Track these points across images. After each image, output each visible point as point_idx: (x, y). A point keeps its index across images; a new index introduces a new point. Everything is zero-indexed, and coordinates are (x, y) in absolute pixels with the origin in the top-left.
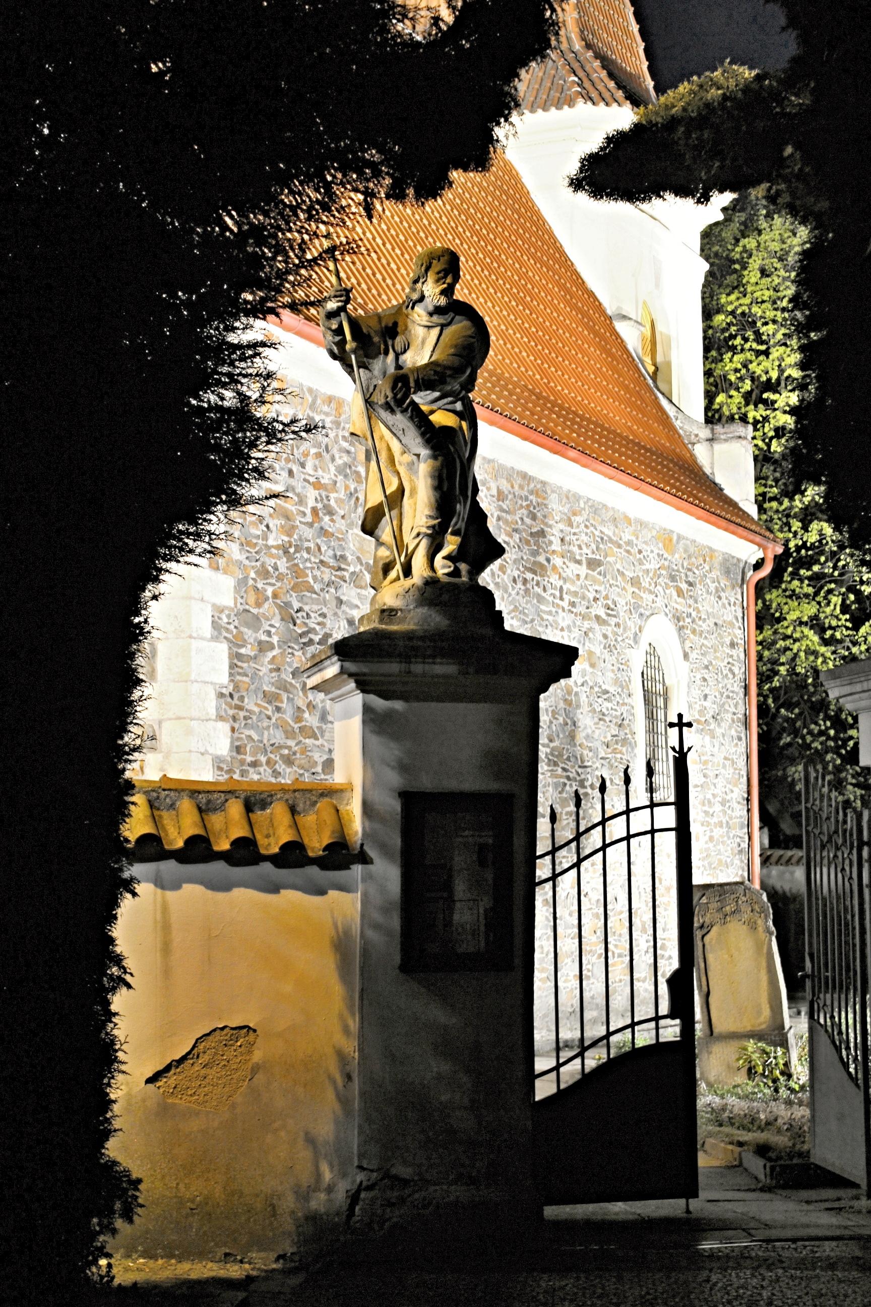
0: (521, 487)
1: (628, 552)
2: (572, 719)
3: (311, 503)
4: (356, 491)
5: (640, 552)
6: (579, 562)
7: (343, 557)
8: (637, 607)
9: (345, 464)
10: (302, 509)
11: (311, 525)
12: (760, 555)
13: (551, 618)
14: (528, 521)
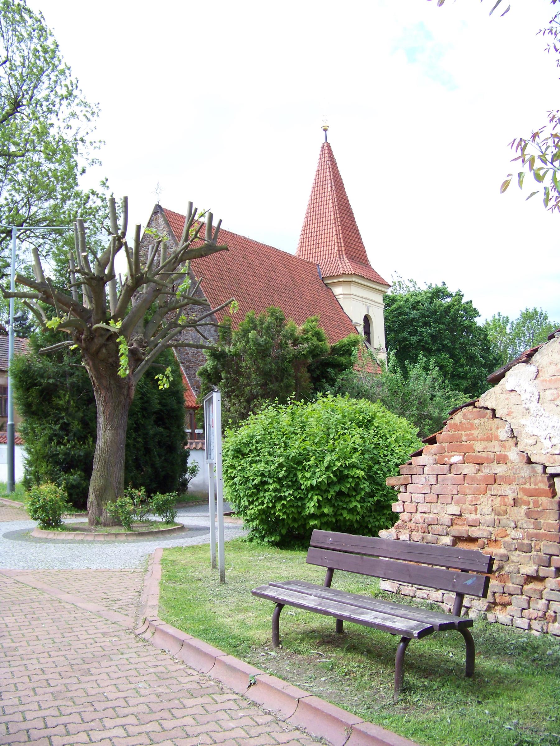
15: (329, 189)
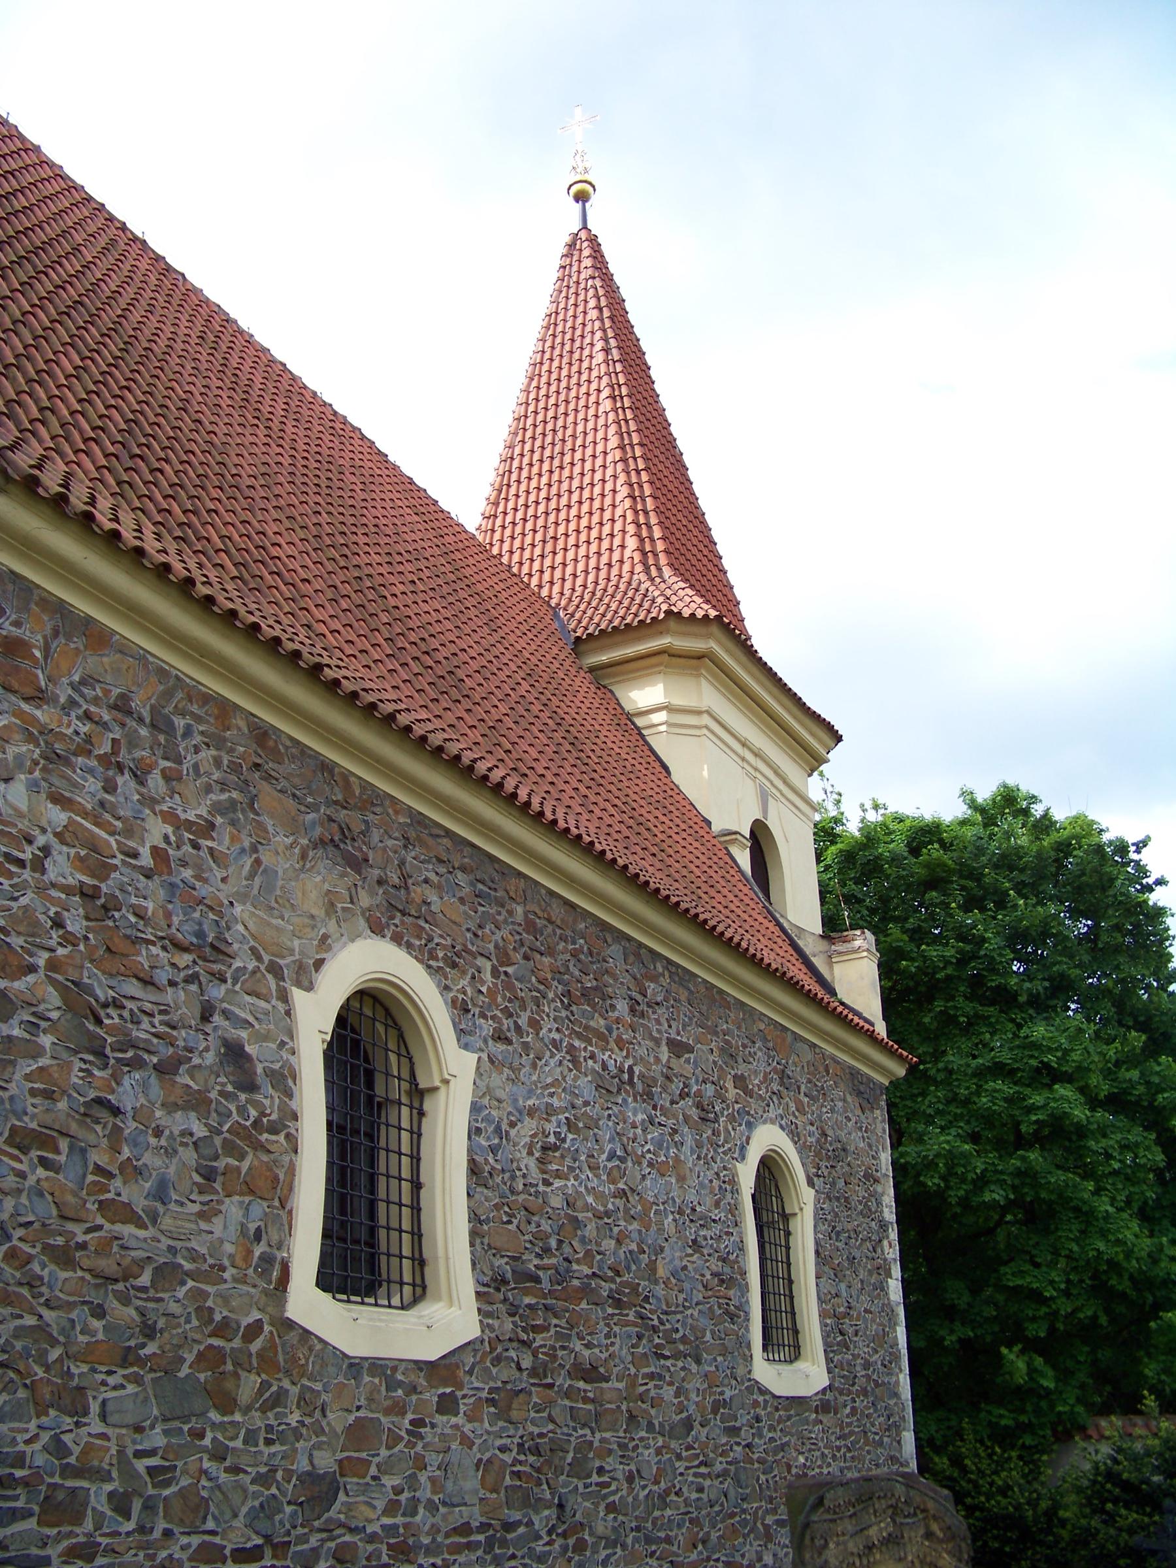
15: (599, 358)
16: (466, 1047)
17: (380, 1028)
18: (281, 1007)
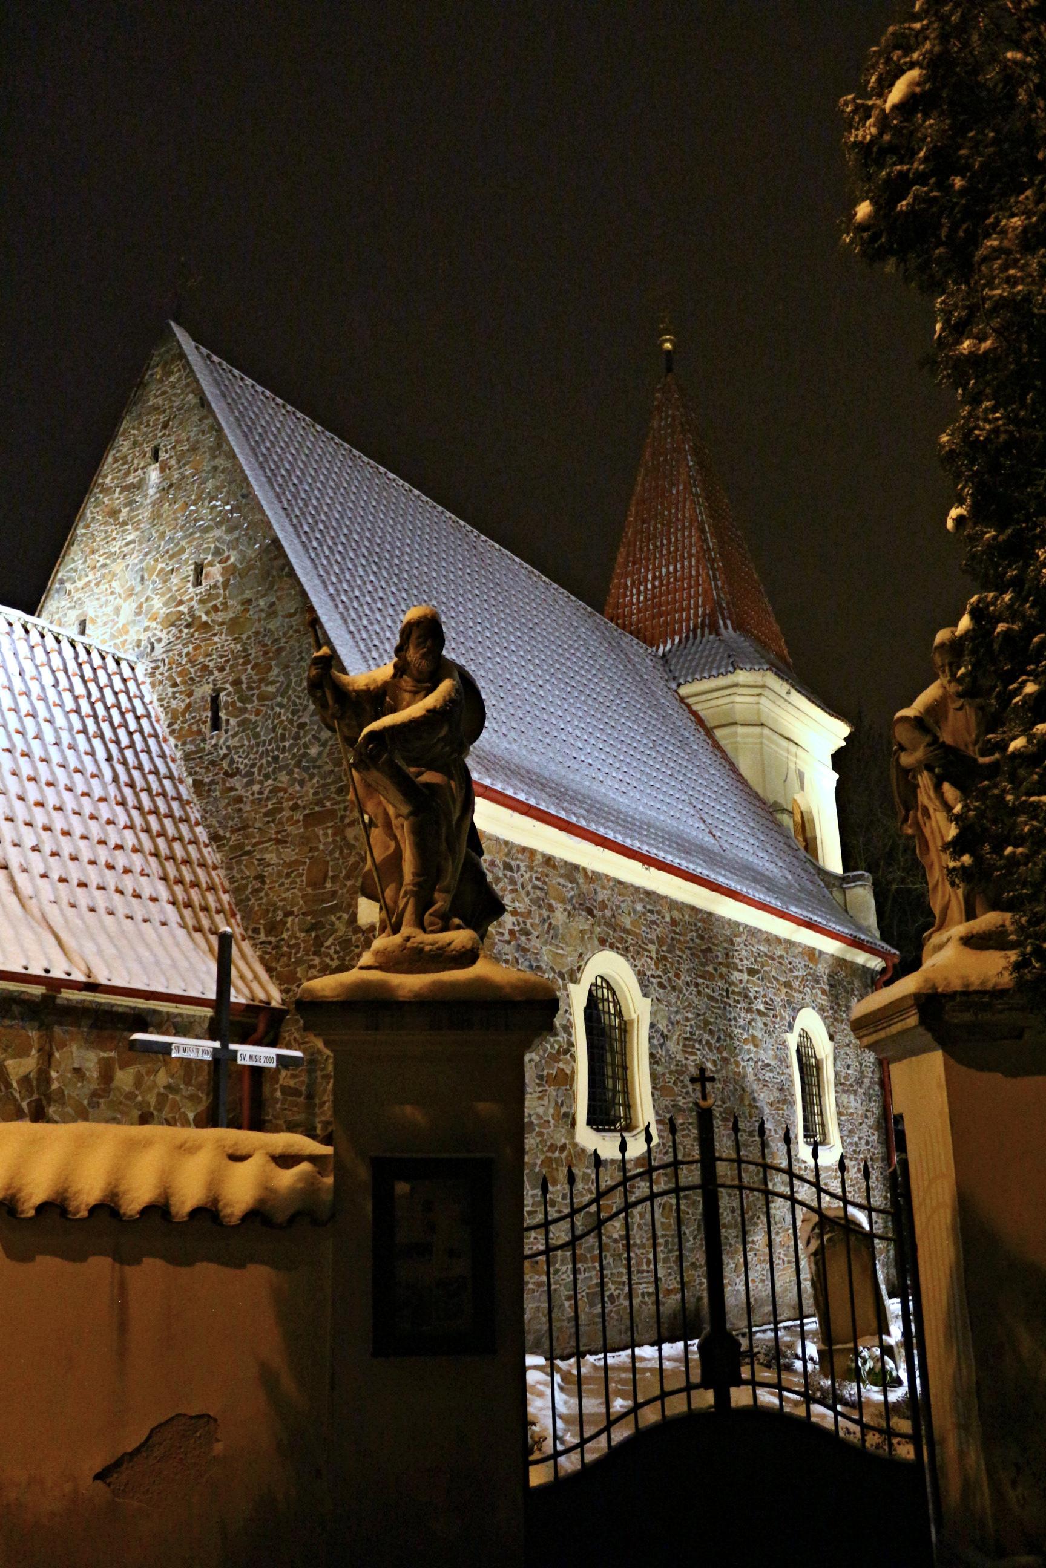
0: (690, 916)
1: (780, 963)
2: (741, 1086)
3: (509, 926)
4: (549, 917)
5: (790, 963)
6: (741, 971)
7: (539, 968)
8: (789, 1003)
9: (539, 898)
10: (501, 930)
11: (509, 942)
12: (883, 964)
13: (719, 1012)
14: (698, 941)
16: (645, 995)
17: (605, 991)
18: (565, 993)
